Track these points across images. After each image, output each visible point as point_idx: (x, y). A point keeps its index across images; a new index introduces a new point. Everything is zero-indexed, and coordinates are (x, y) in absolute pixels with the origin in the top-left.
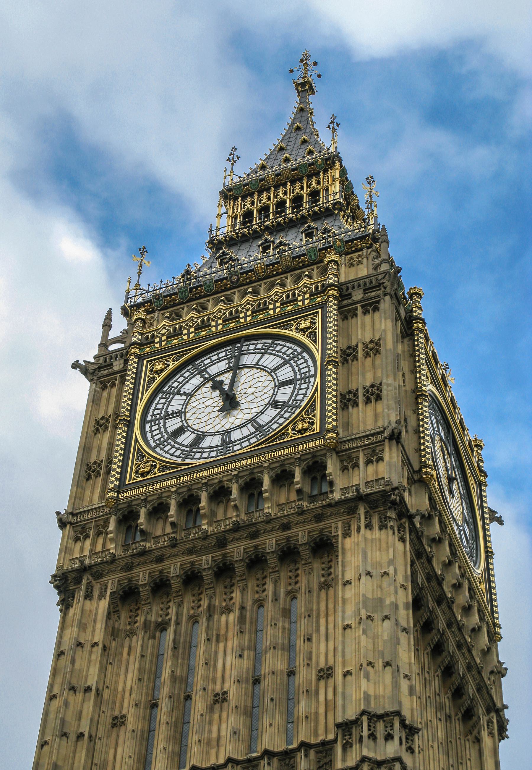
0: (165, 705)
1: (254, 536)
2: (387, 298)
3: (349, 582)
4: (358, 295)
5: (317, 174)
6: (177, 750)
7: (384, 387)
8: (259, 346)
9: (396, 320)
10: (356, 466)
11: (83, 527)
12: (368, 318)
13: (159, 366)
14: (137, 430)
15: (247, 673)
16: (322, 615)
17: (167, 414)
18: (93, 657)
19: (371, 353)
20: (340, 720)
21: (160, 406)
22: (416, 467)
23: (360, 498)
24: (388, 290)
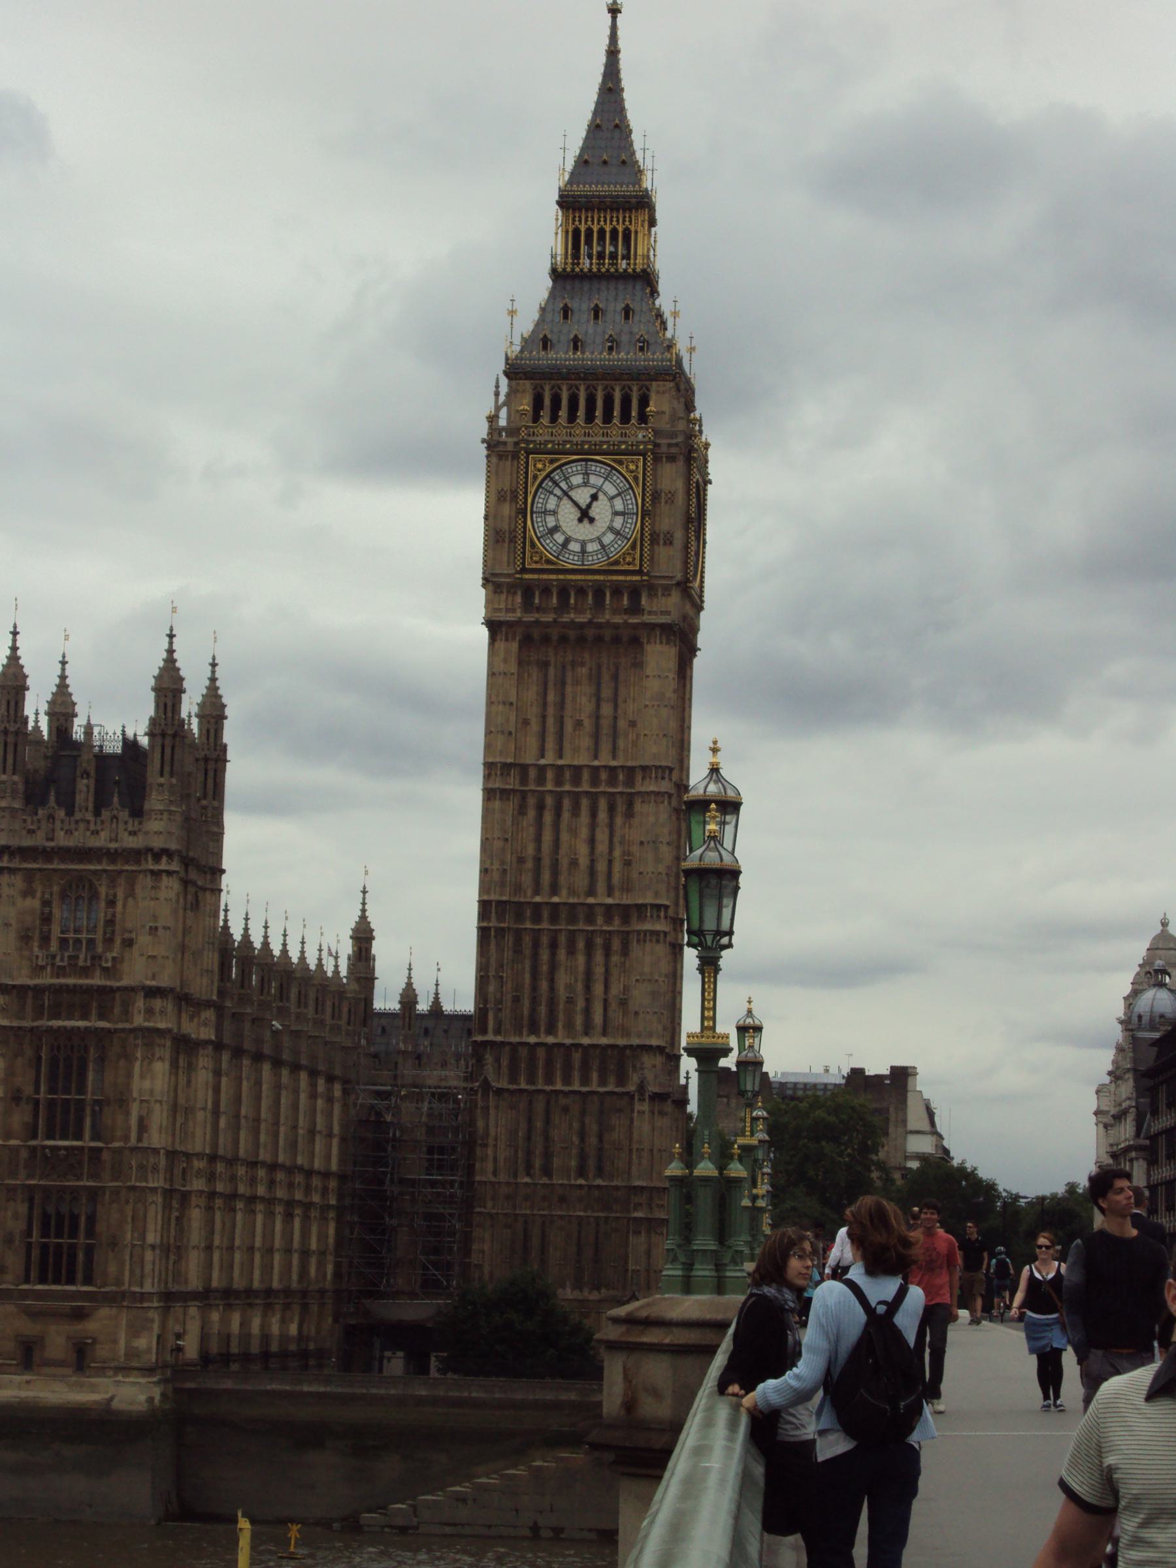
0: (550, 721)
4: (664, 449)
5: (630, 210)
10: (656, 595)
13: (540, 466)
14: (529, 522)
17: (546, 510)
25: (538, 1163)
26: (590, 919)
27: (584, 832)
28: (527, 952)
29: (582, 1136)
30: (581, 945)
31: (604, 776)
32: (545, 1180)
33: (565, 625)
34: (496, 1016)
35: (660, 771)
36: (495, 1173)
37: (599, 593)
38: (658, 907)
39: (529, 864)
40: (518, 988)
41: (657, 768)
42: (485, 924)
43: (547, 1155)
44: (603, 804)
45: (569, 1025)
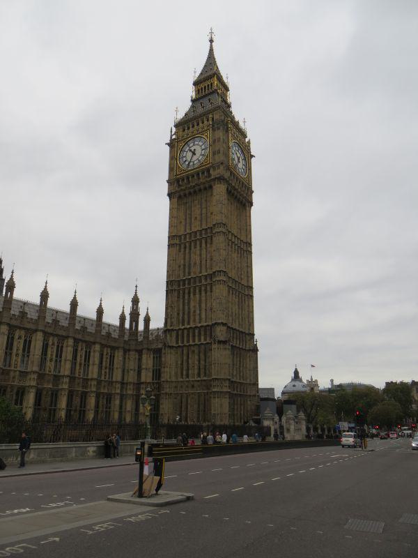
0: (188, 219)
25: (184, 373)
26: (200, 281)
27: (198, 252)
28: (181, 297)
29: (199, 361)
30: (197, 291)
31: (203, 232)
32: (187, 379)
33: (189, 188)
36: (170, 378)
37: (198, 174)
38: (220, 271)
39: (182, 267)
40: (179, 310)
43: (188, 369)
44: (203, 241)
45: (194, 321)
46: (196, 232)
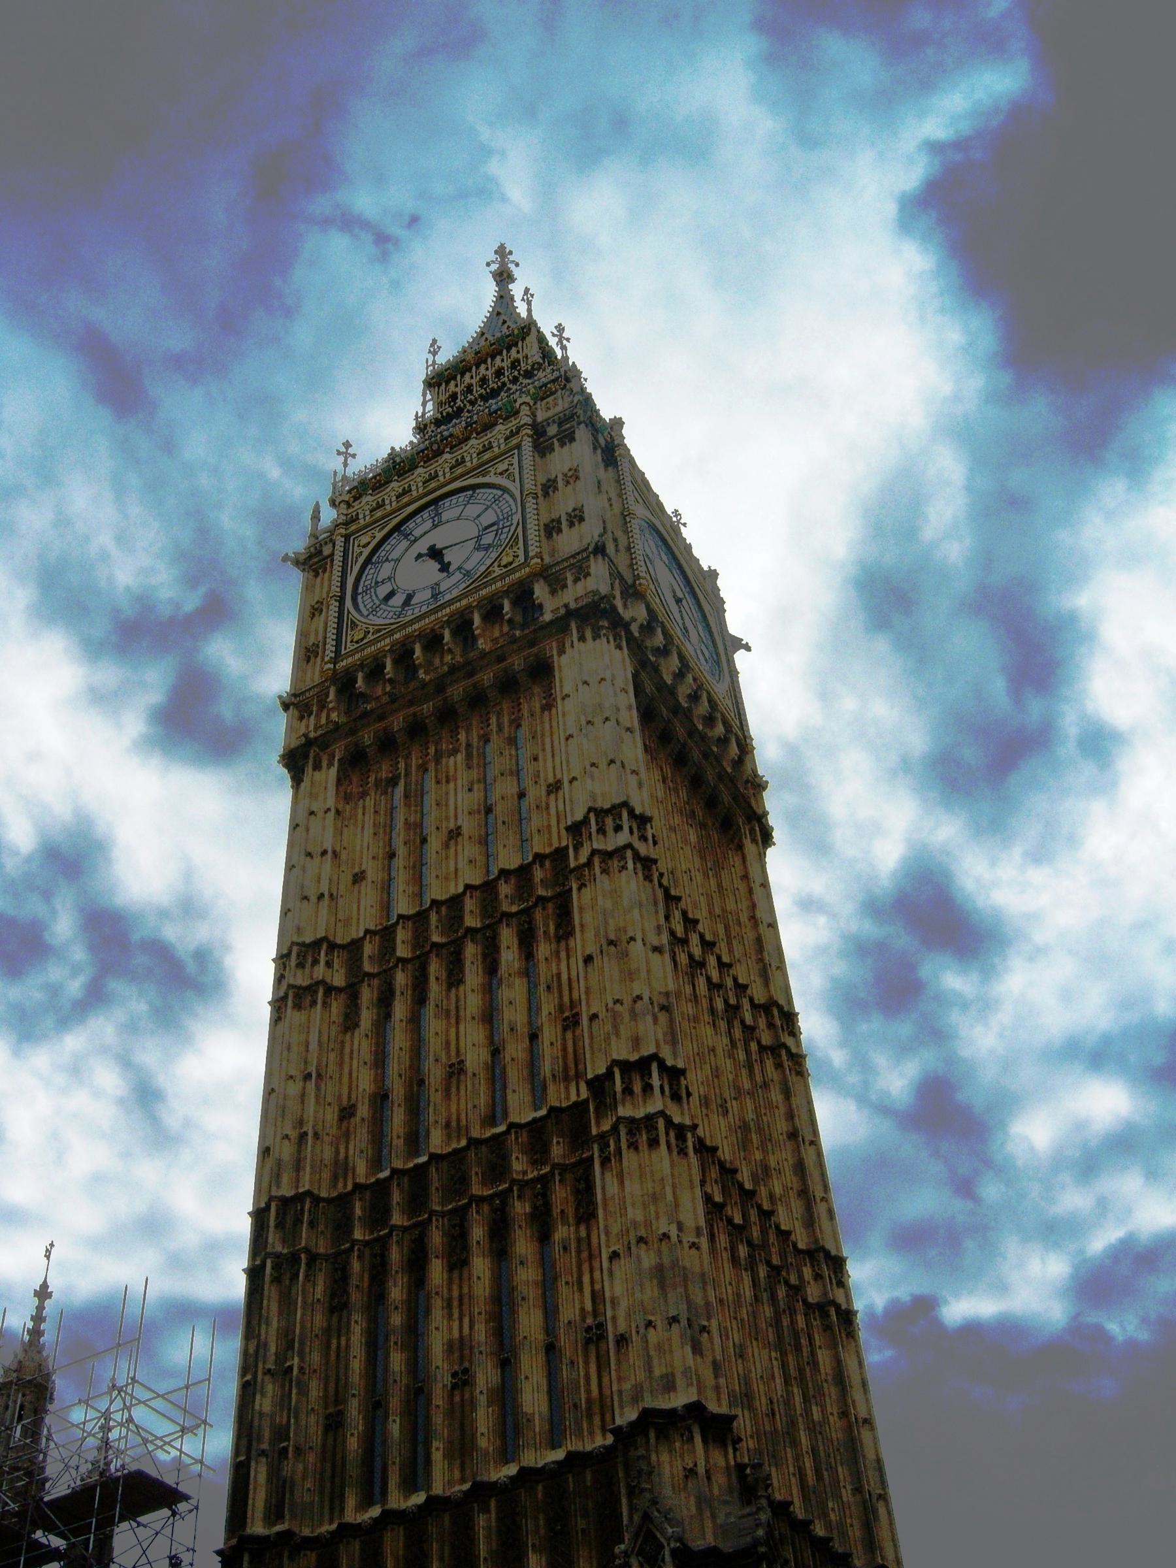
1: (471, 675)
2: (583, 426)
3: (568, 696)
4: (552, 430)
5: (516, 345)
6: (417, 889)
7: (585, 509)
8: (461, 499)
9: (595, 449)
10: (565, 586)
11: (307, 705)
12: (566, 448)
13: (364, 540)
15: (479, 805)
16: (547, 734)
17: (377, 583)
18: (327, 821)
19: (571, 481)
20: (569, 823)
21: (370, 577)
22: (630, 582)
23: (570, 614)
24: (582, 419)
26: (497, 1169)
27: (473, 1002)
30: (478, 1233)
31: (505, 889)
34: (274, 1473)
35: (609, 822)
38: (643, 1065)
39: (363, 1111)
41: (601, 813)
42: (258, 1263)
44: (508, 937)
45: (462, 1449)
46: (455, 902)
